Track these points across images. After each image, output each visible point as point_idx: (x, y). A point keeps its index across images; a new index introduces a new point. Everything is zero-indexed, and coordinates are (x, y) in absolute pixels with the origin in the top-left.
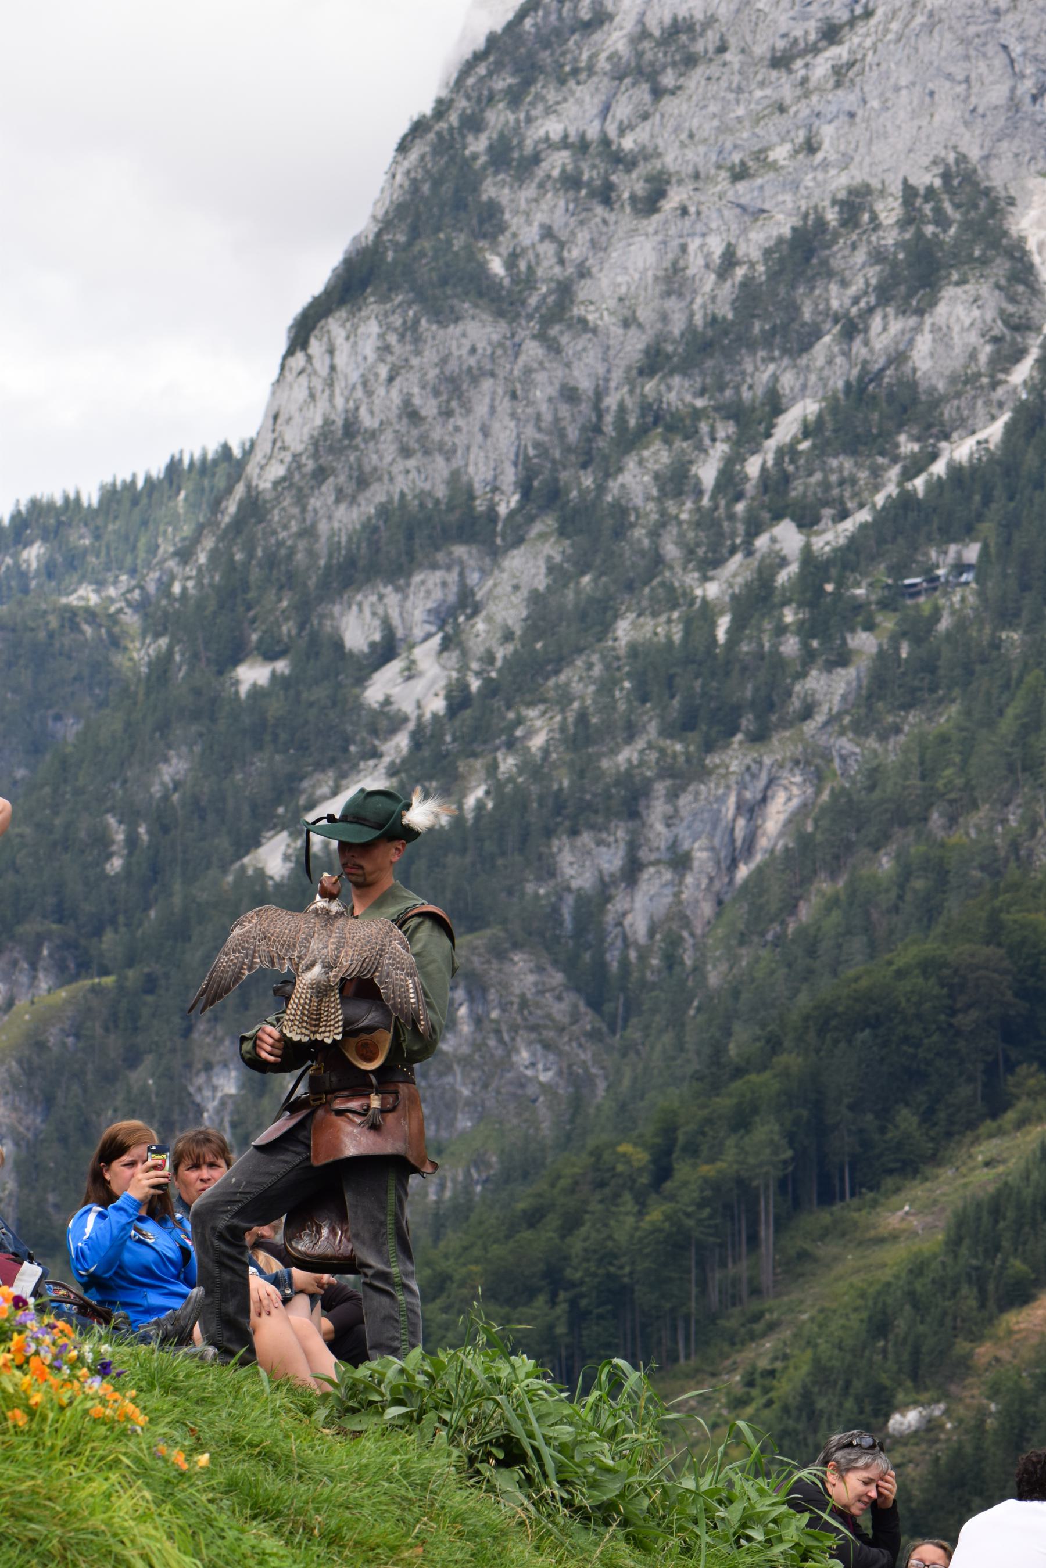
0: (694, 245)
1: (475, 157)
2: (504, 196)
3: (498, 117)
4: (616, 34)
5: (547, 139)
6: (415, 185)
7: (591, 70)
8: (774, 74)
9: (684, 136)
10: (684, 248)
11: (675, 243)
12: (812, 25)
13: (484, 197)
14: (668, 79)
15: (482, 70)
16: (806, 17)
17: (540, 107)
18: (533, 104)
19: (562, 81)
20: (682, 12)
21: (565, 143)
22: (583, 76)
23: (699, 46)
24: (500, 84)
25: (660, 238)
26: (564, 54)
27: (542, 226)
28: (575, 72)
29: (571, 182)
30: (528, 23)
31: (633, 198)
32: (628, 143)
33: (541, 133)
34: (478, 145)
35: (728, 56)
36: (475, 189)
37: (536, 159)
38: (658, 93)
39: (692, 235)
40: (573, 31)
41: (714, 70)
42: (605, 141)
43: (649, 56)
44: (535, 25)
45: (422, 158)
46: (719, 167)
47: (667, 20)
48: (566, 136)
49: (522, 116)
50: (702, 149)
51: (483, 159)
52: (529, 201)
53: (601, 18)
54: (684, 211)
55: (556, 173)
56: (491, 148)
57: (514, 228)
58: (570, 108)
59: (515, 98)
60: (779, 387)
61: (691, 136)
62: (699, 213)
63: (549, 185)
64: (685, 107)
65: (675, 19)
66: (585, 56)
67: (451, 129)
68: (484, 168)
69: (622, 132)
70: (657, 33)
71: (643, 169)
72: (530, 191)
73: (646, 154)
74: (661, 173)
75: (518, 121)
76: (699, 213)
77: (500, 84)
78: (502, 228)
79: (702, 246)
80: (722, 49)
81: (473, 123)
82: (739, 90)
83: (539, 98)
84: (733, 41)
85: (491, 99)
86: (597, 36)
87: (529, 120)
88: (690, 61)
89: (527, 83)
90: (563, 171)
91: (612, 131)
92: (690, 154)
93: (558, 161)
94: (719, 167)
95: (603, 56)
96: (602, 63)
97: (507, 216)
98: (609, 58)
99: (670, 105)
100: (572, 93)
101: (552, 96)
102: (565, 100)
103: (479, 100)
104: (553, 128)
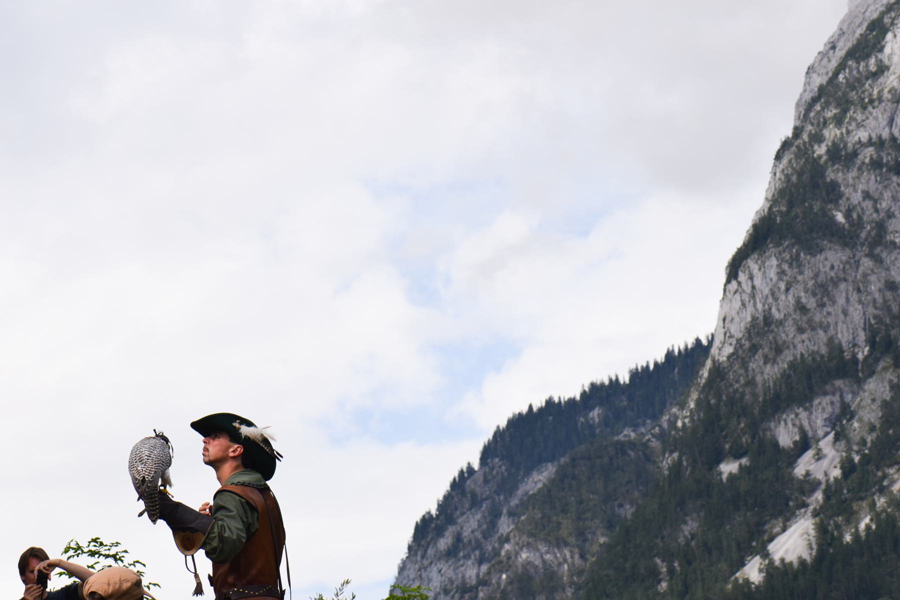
1: (820, 157)
3: (831, 133)
4: (892, 77)
5: (860, 141)
6: (788, 177)
7: (880, 99)
13: (828, 180)
15: (818, 107)
17: (854, 124)
18: (849, 123)
19: (864, 108)
21: (870, 143)
22: (876, 103)
24: (829, 114)
26: (863, 92)
27: (863, 192)
28: (871, 101)
29: (876, 164)
30: (841, 77)
33: (856, 139)
34: (821, 150)
36: (823, 175)
37: (855, 154)
40: (867, 79)
44: (845, 78)
45: (790, 161)
48: (870, 139)
49: (844, 131)
52: (854, 179)
55: (867, 161)
56: (828, 151)
57: (847, 195)
58: (871, 122)
59: (839, 121)
63: (864, 168)
66: (875, 92)
68: (826, 162)
72: (854, 173)
75: (842, 134)
77: (829, 114)
78: (840, 196)
81: (817, 138)
85: (825, 123)
86: (881, 80)
87: (848, 132)
89: (845, 111)
90: (871, 159)
93: (868, 153)
95: (886, 91)
96: (886, 95)
97: (842, 189)
98: (890, 92)
100: (871, 114)
101: (859, 117)
102: (867, 118)
103: (818, 124)
104: (863, 135)
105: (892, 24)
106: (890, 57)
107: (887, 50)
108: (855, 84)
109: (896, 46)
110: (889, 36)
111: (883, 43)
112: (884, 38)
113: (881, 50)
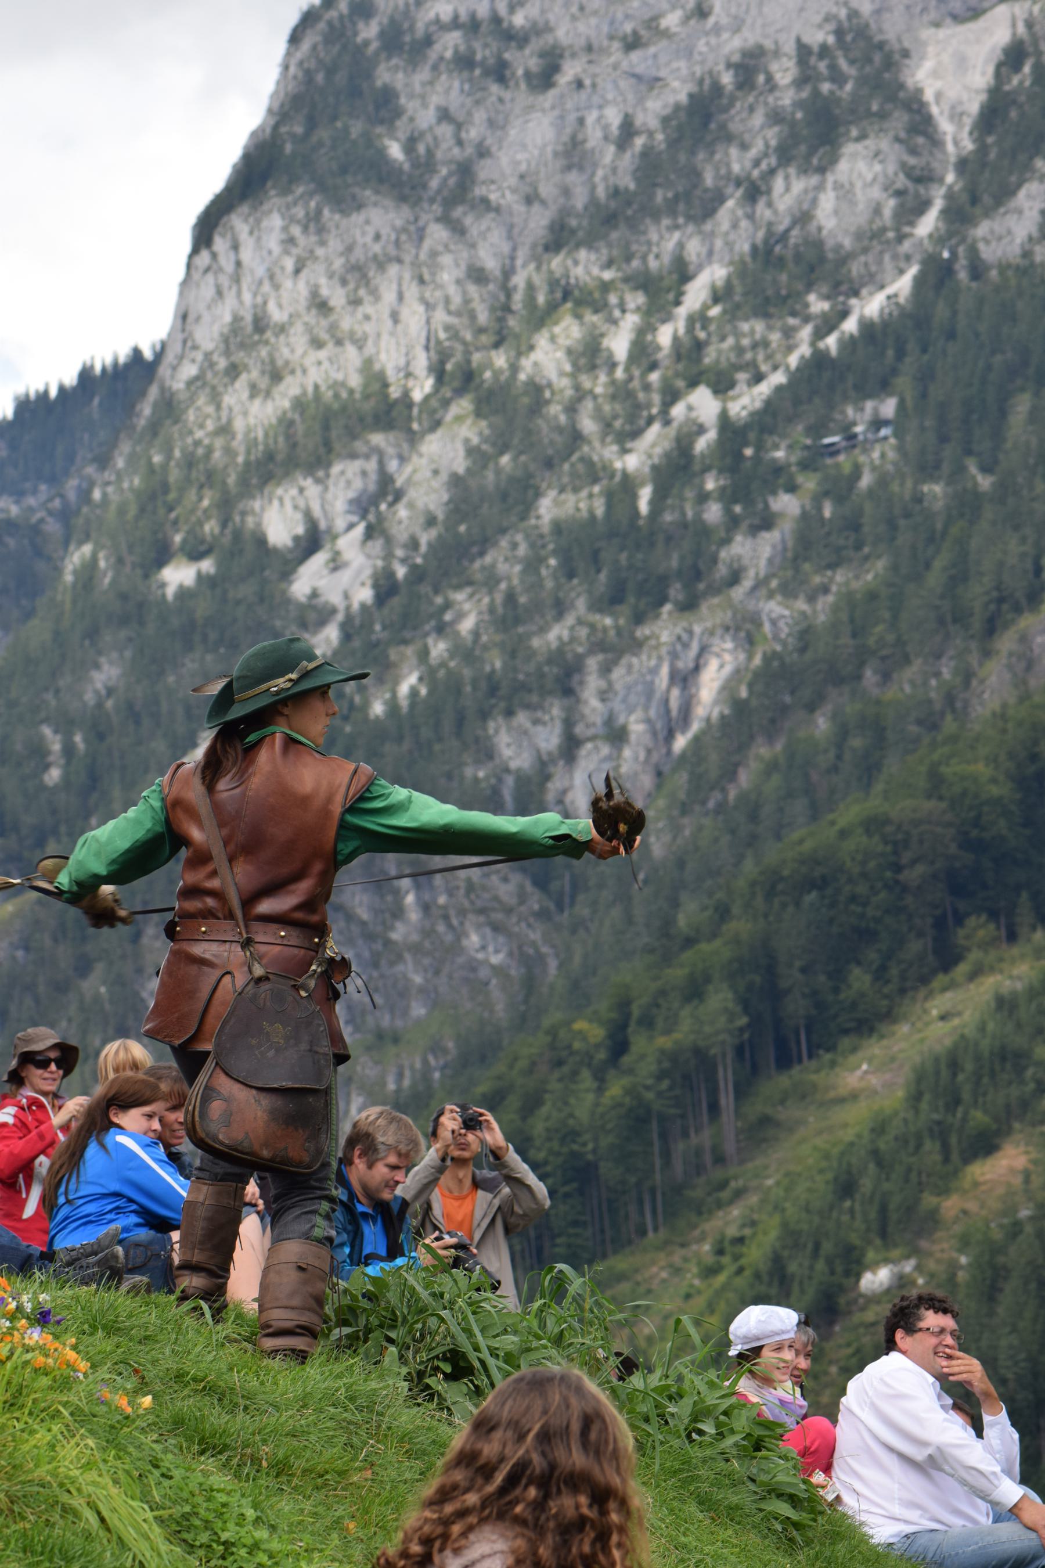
0: (591, 118)
1: (367, 43)
2: (399, 81)
5: (437, 21)
6: (309, 76)
9: (574, 9)
10: (581, 121)
11: (572, 117)
13: (379, 83)
21: (455, 23)
25: (556, 113)
29: (464, 62)
31: (528, 75)
32: (519, 20)
33: (432, 15)
34: (369, 31)
37: (428, 41)
39: (589, 107)
42: (496, 19)
45: (314, 48)
46: (611, 38)
48: (456, 17)
50: (593, 21)
51: (374, 46)
52: (424, 84)
54: (579, 84)
55: (449, 54)
56: (382, 34)
57: (410, 113)
60: (685, 254)
61: (582, 8)
62: (594, 85)
63: (443, 67)
67: (341, 17)
68: (377, 53)
71: (535, 44)
72: (423, 75)
74: (555, 47)
76: (594, 85)
78: (398, 113)
79: (599, 119)
90: (456, 52)
92: (581, 27)
93: (450, 42)
97: (403, 100)
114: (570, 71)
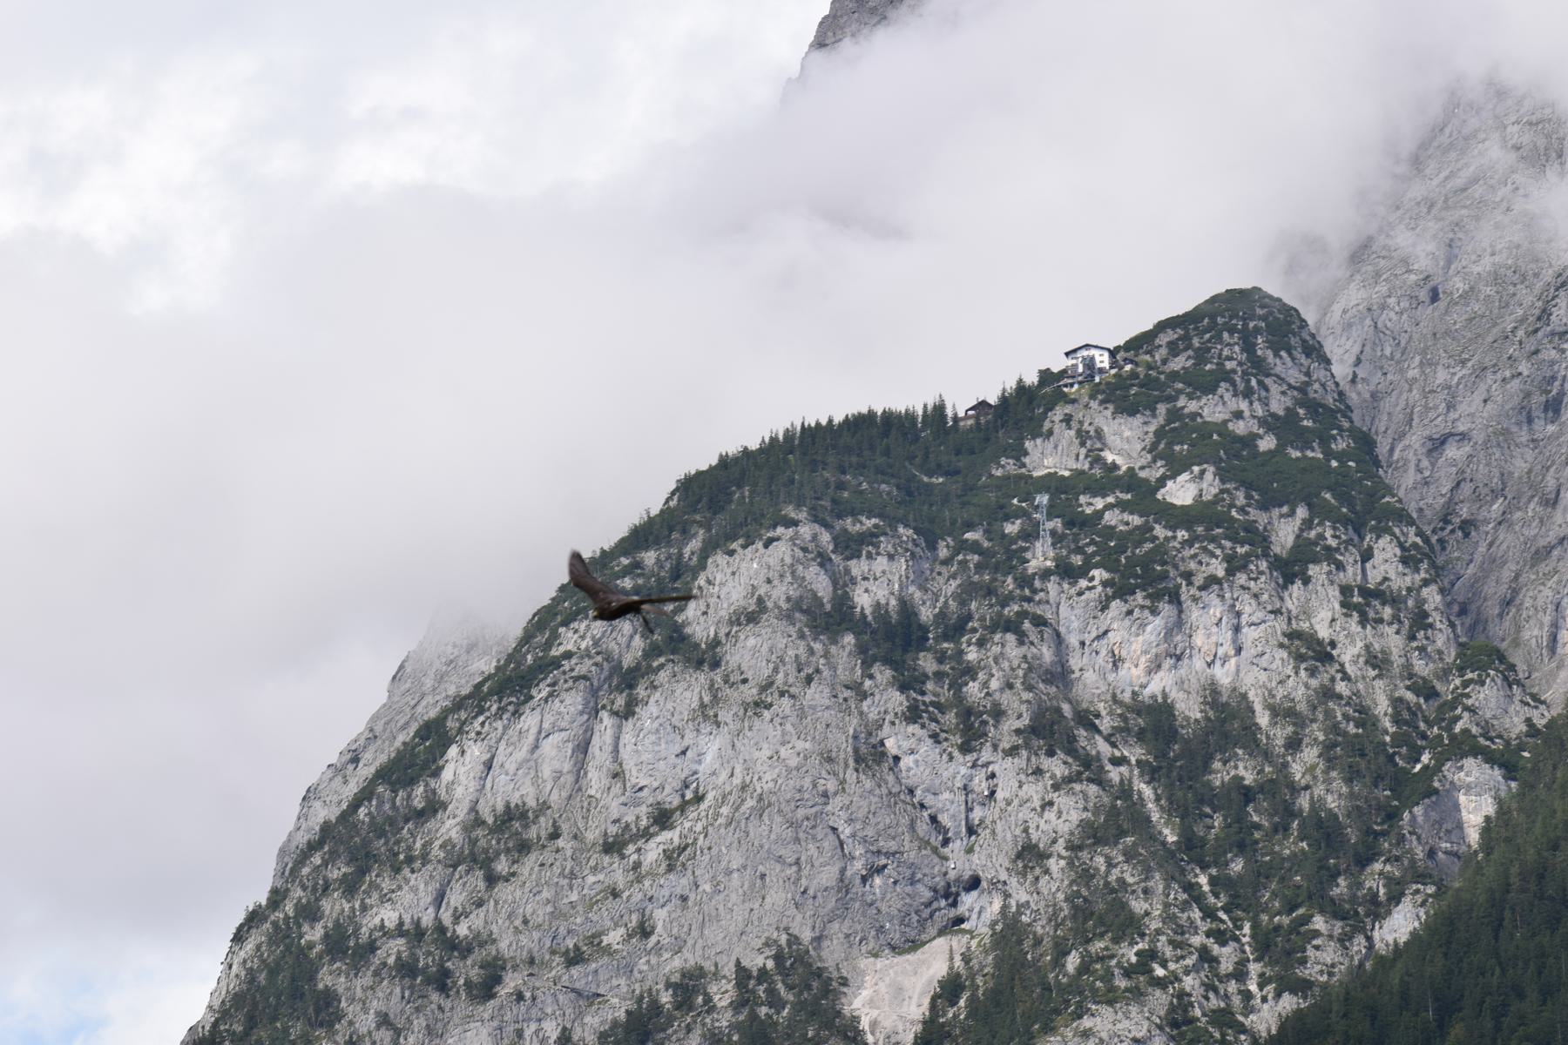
1: (311, 946)
3: (334, 906)
5: (382, 926)
8: (607, 859)
9: (518, 923)
12: (643, 810)
13: (321, 986)
14: (502, 866)
15: (317, 860)
16: (637, 804)
17: (375, 895)
18: (368, 893)
19: (397, 870)
20: (515, 800)
21: (400, 931)
22: (417, 864)
23: (532, 833)
24: (334, 874)
25: (495, 1023)
26: (398, 842)
27: (378, 1014)
28: (410, 860)
29: (406, 969)
30: (362, 812)
31: (469, 984)
32: (462, 930)
33: (377, 921)
34: (314, 934)
35: (560, 843)
36: (312, 978)
37: (372, 947)
38: (492, 880)
40: (407, 821)
41: (547, 857)
42: (440, 929)
43: (482, 843)
44: (369, 813)
45: (258, 947)
46: (553, 952)
47: (500, 807)
48: (401, 924)
50: (536, 935)
53: (435, 806)
54: (520, 997)
55: (391, 961)
56: (326, 935)
58: (405, 896)
59: (350, 887)
61: (525, 922)
62: (534, 998)
63: (384, 973)
64: (518, 893)
65: (507, 806)
66: (418, 845)
67: (287, 918)
68: (320, 956)
69: (457, 919)
70: (490, 820)
71: (478, 955)
72: (367, 979)
73: (482, 940)
74: (496, 958)
75: (353, 909)
76: (534, 998)
79: (537, 1032)
80: (555, 835)
81: (309, 913)
82: (572, 876)
83: (374, 886)
84: (565, 827)
85: (326, 888)
87: (364, 908)
88: (524, 847)
89: (362, 872)
90: (399, 958)
91: (446, 917)
92: (524, 940)
93: (393, 949)
94: (553, 952)
95: (437, 843)
96: (436, 852)
97: (343, 1004)
99: (504, 891)
100: (407, 881)
101: (386, 884)
102: (400, 888)
103: (314, 889)
104: (389, 916)
105: (460, 731)
106: (450, 787)
107: (447, 775)
108: (386, 827)
109: (462, 770)
110: (453, 751)
111: (441, 763)
112: (443, 754)
113: (436, 773)
114: (511, 982)
